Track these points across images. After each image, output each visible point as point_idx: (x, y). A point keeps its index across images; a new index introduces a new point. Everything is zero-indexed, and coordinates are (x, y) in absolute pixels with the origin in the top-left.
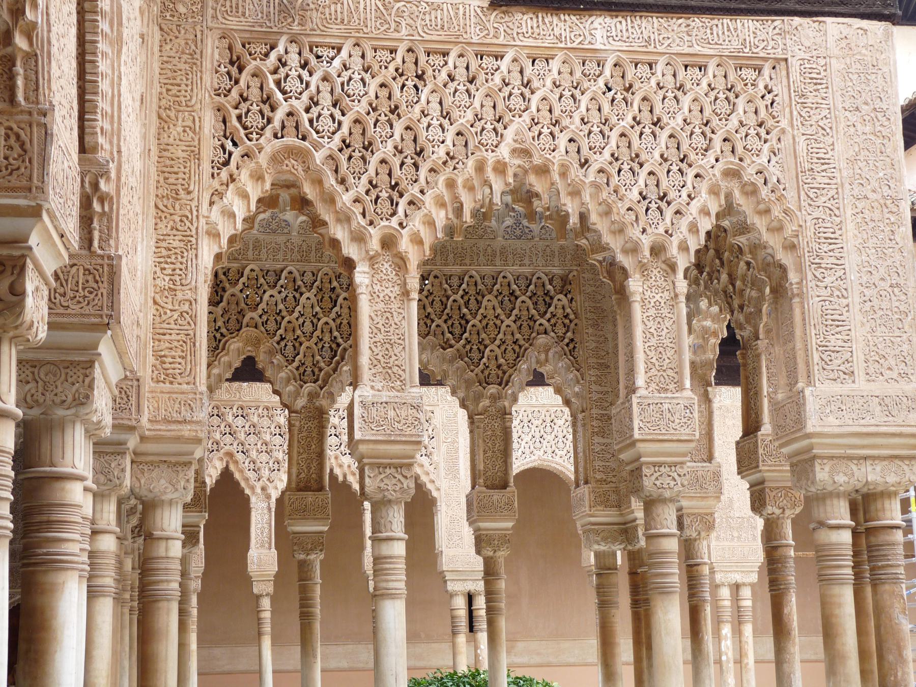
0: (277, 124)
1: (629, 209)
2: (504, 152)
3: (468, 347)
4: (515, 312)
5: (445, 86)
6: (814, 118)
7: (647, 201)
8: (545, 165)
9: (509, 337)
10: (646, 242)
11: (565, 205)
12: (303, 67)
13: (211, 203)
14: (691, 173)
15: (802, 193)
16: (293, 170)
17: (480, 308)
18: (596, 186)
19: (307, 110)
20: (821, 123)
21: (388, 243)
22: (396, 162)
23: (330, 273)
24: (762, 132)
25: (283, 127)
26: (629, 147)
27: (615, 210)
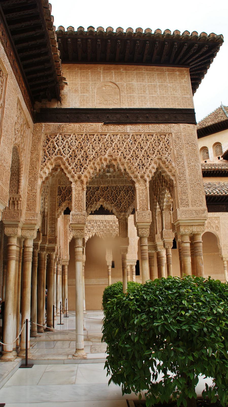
0: (56, 152)
1: (135, 168)
2: (106, 156)
3: (117, 203)
4: (128, 195)
5: (93, 142)
6: (178, 146)
9: (127, 201)
10: (139, 175)
12: (62, 140)
13: (41, 170)
14: (150, 159)
15: (176, 163)
18: (128, 163)
19: (63, 149)
20: (180, 147)
21: (79, 177)
24: (166, 149)
25: (57, 153)
26: (135, 154)
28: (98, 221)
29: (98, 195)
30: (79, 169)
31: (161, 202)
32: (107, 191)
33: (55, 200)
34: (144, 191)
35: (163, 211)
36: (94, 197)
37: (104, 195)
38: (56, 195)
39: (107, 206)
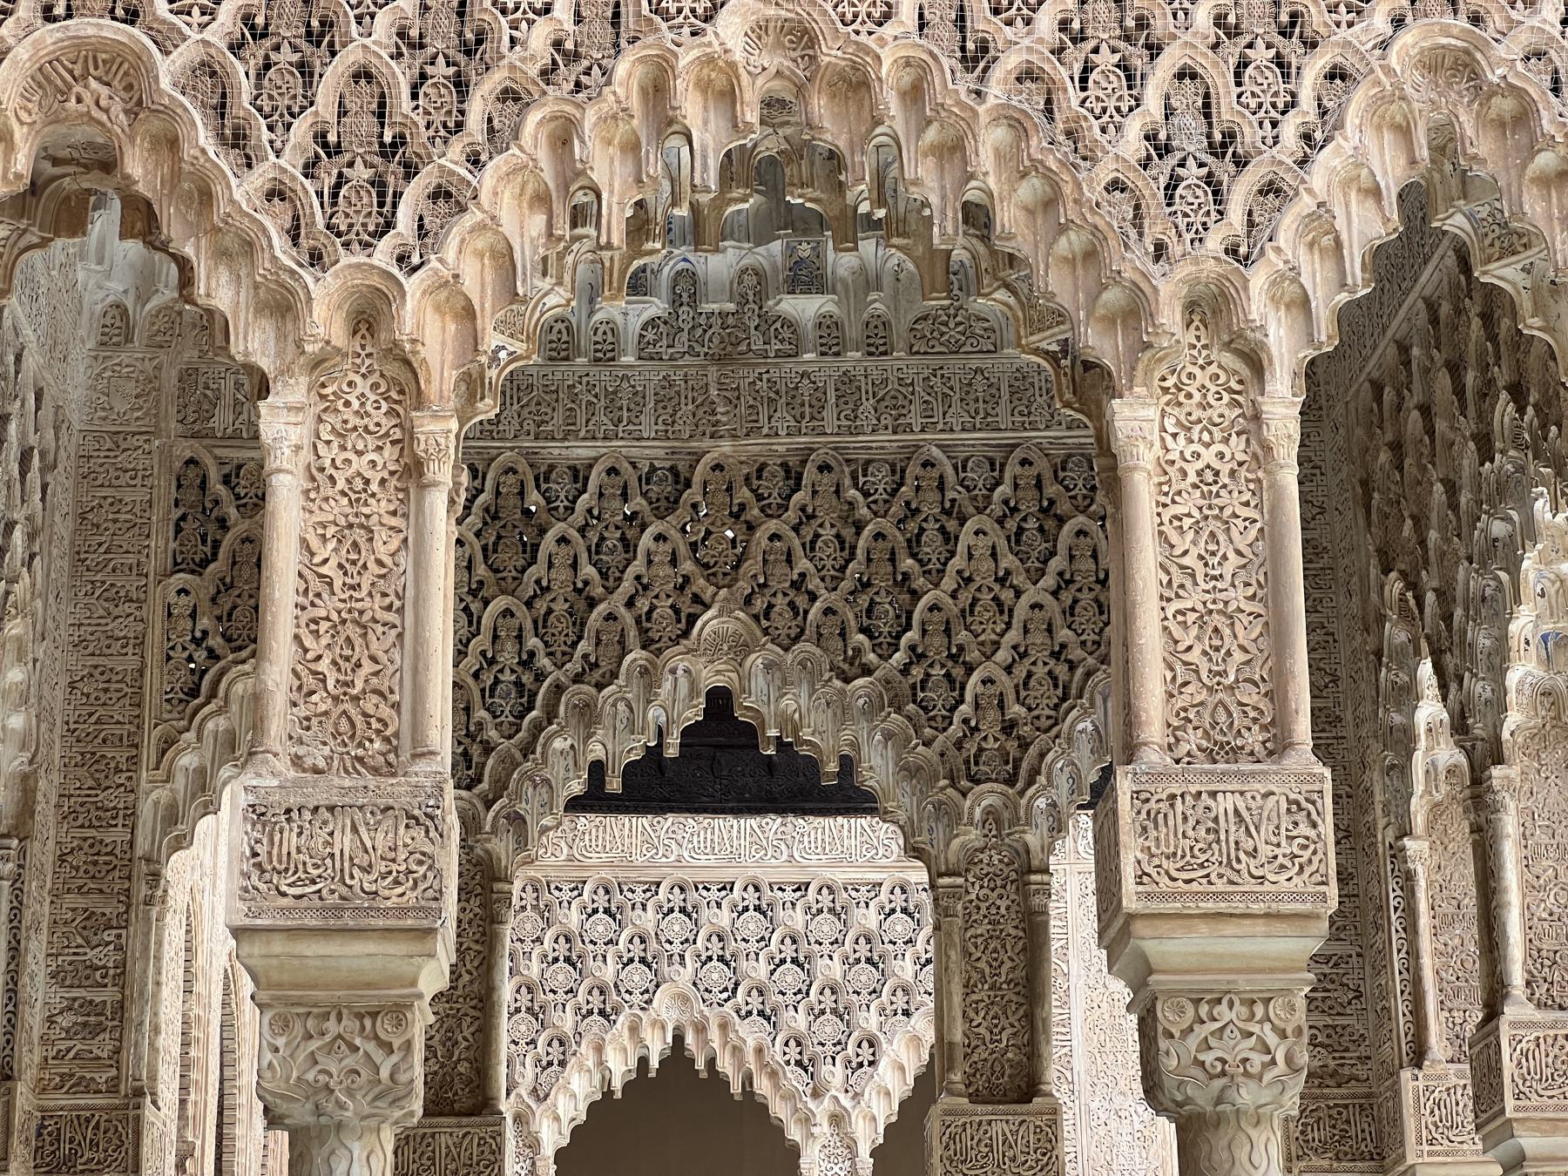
1: (1115, 186)
3: (917, 672)
4: (1055, 564)
7: (1172, 160)
8: (855, 67)
9: (1038, 638)
11: (916, 182)
14: (1313, 68)
16: (96, 113)
17: (953, 554)
22: (400, 77)
23: (522, 466)
27: (1068, 189)
28: (714, 895)
29: (674, 562)
30: (360, 209)
31: (1467, 648)
32: (792, 515)
33: (130, 629)
34: (1232, 502)
35: (1496, 772)
36: (627, 586)
37: (752, 566)
38: (151, 567)
39: (788, 703)
